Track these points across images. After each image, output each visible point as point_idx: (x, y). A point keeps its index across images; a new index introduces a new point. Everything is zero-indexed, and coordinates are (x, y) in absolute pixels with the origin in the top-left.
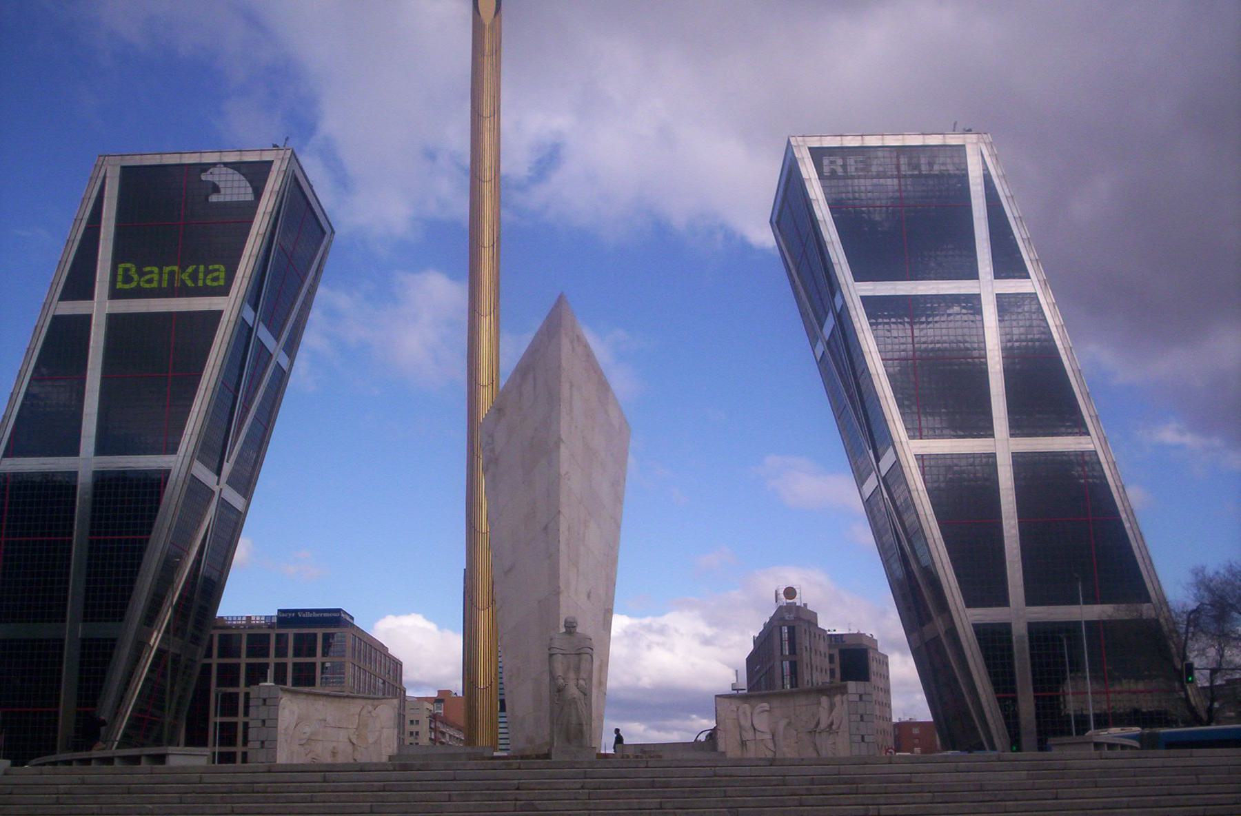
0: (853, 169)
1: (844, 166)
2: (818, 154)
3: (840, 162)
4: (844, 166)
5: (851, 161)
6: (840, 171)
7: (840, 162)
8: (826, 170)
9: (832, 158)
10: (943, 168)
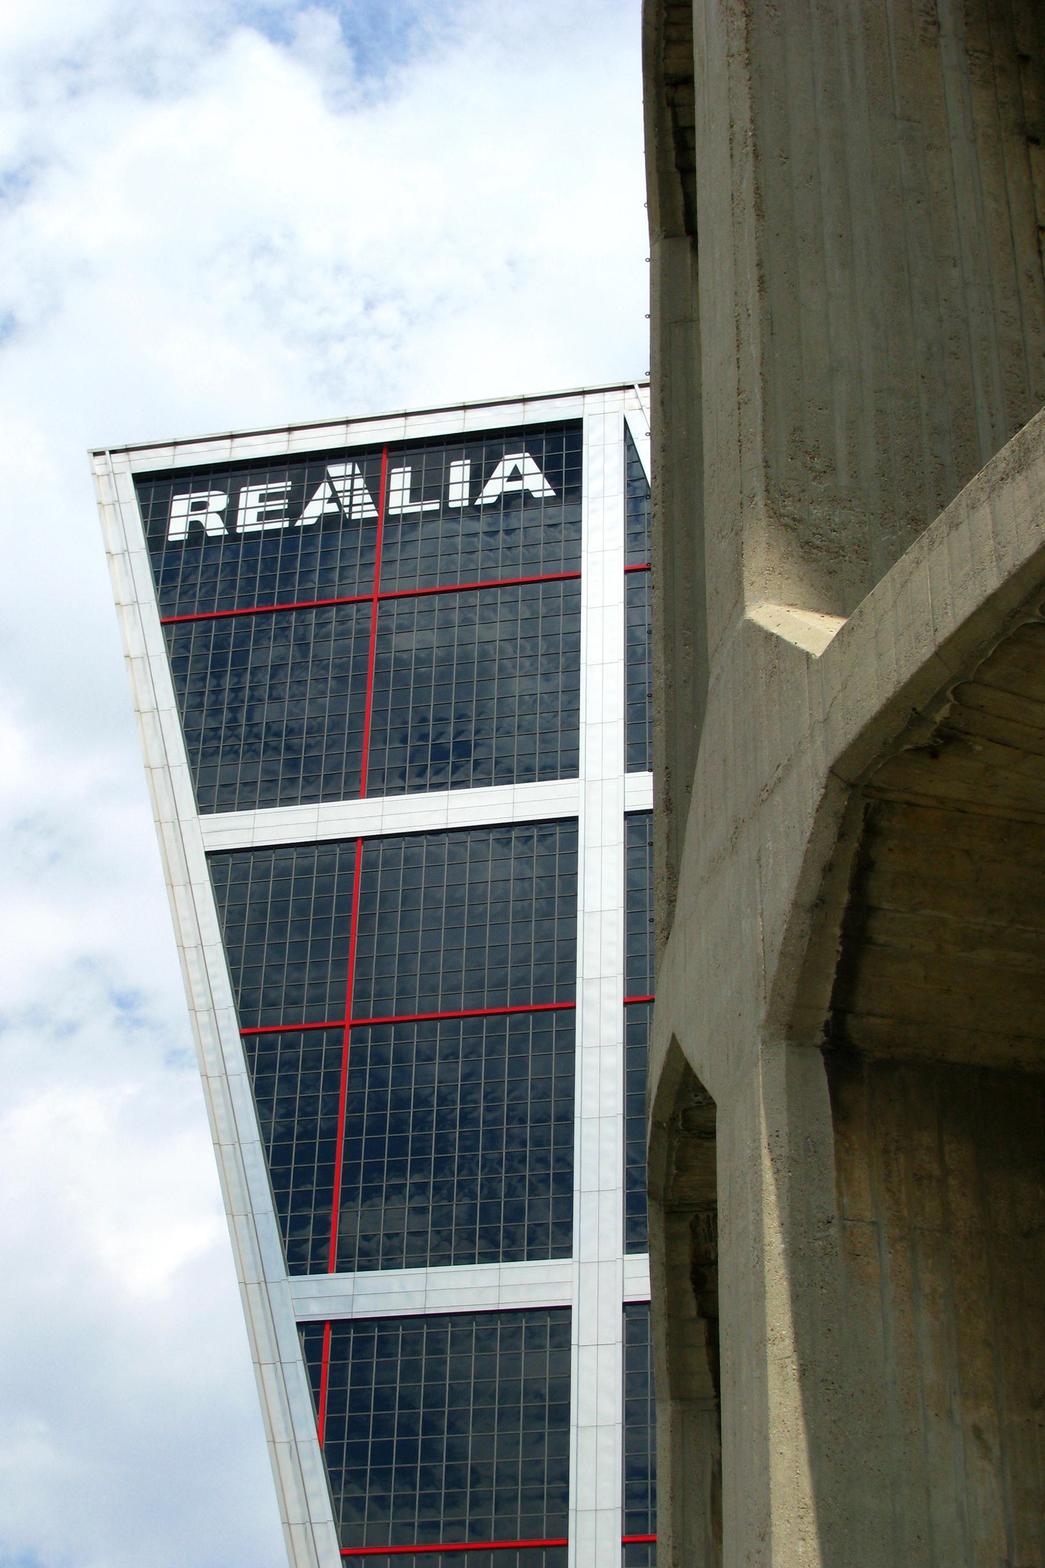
0: (252, 516)
1: (229, 515)
2: (155, 488)
3: (218, 501)
4: (229, 515)
5: (250, 498)
6: (214, 526)
7: (218, 501)
8: (177, 529)
9: (199, 496)
10: (515, 486)
